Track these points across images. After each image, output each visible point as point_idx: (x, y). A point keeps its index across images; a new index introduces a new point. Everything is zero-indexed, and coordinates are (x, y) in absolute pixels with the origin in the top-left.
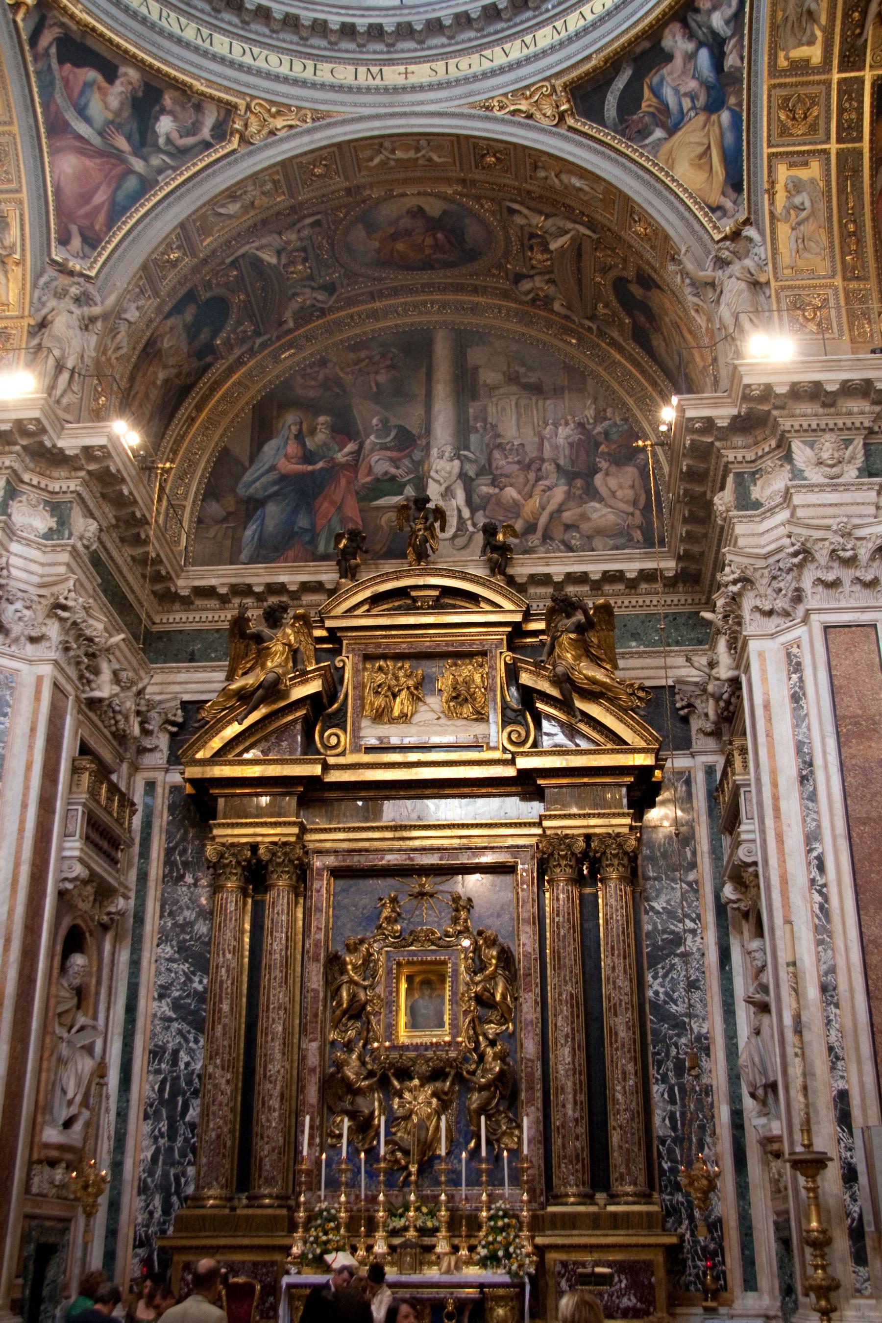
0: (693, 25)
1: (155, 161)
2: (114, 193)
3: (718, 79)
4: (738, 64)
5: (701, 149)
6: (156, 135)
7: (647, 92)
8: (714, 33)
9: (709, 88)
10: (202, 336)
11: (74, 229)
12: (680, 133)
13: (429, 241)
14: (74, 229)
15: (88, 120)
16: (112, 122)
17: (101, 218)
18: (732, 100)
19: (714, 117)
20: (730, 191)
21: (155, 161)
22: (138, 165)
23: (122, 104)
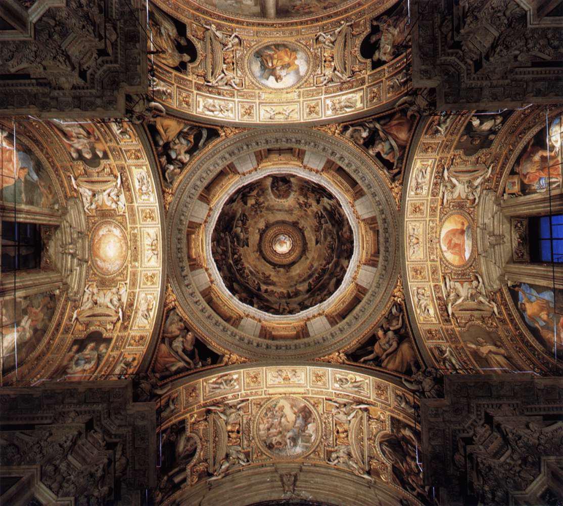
0: (180, 164)
1: (371, 125)
2: (389, 121)
3: (167, 152)
4: (161, 160)
5: (169, 130)
6: (369, 132)
7: (192, 140)
8: (171, 164)
9: (170, 149)
10: (374, 39)
11: (408, 117)
12: (178, 132)
13: (275, 62)
14: (408, 117)
15: (391, 144)
16: (383, 141)
17: (398, 116)
18: (160, 149)
19: (165, 141)
20: (153, 123)
21: (371, 125)
22: (378, 126)
23: (378, 145)
